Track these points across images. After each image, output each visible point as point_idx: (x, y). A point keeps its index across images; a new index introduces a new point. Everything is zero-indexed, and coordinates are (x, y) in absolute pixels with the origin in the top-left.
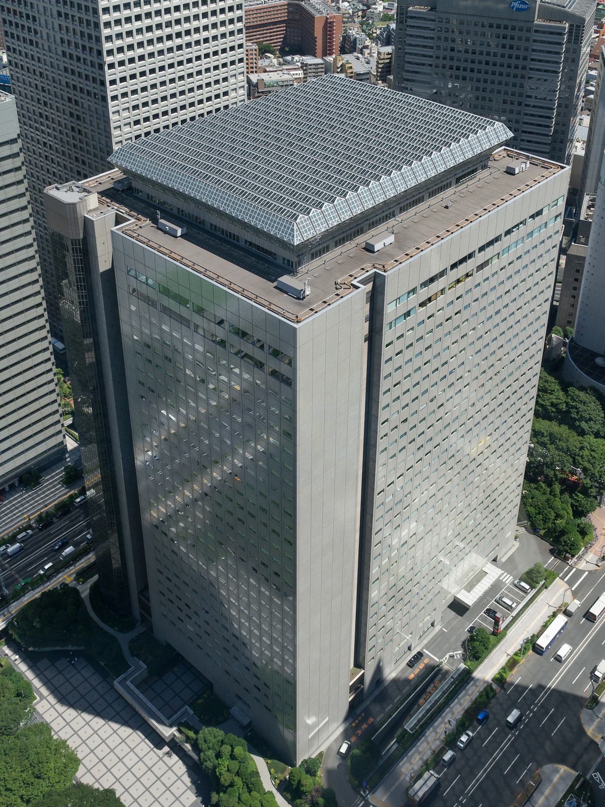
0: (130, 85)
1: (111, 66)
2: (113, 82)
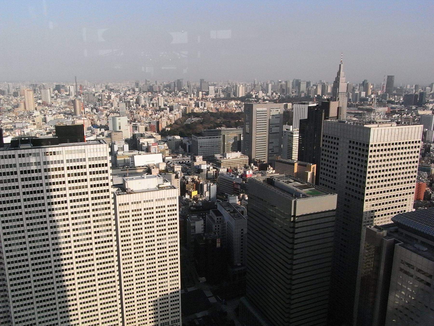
0: (373, 196)
1: (368, 188)
2: (367, 194)
